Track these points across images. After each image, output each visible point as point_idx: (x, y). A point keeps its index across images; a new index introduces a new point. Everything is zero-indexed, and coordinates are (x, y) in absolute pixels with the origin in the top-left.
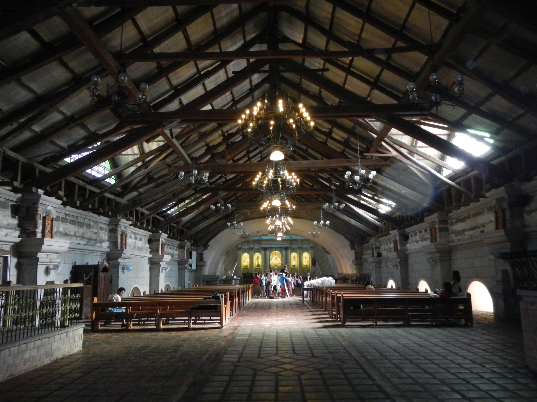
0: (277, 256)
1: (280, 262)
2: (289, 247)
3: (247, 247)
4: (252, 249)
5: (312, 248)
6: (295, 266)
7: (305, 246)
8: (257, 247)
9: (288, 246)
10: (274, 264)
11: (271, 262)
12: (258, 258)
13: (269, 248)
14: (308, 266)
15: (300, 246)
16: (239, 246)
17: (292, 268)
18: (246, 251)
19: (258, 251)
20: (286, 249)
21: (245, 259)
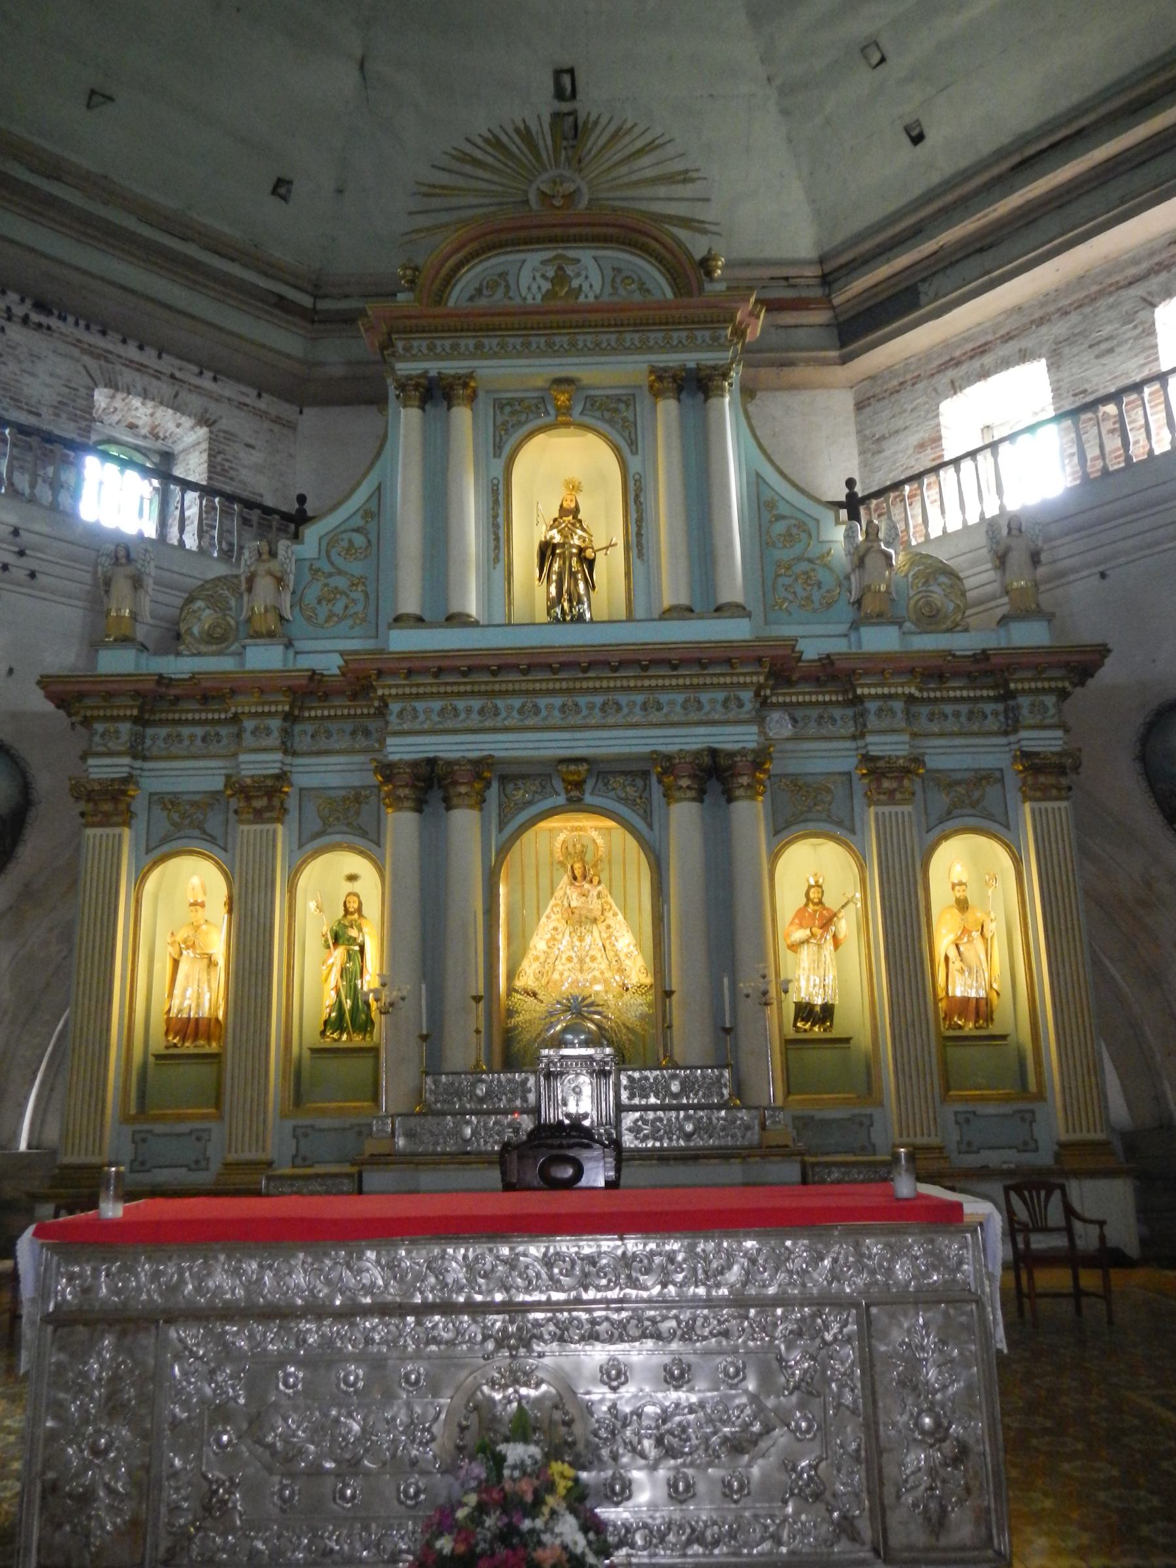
0: (594, 898)
1: (638, 971)
2: (759, 759)
3: (198, 776)
4: (263, 799)
5: (1047, 775)
6: (826, 1013)
7: (950, 755)
8: (330, 771)
9: (738, 738)
10: (549, 997)
11: (528, 977)
12: (352, 912)
13: (482, 770)
14: (1012, 1017)
15: (889, 745)
16: (104, 769)
17: (789, 1043)
18: (185, 825)
19: (346, 821)
20: (715, 776)
21: (174, 930)
